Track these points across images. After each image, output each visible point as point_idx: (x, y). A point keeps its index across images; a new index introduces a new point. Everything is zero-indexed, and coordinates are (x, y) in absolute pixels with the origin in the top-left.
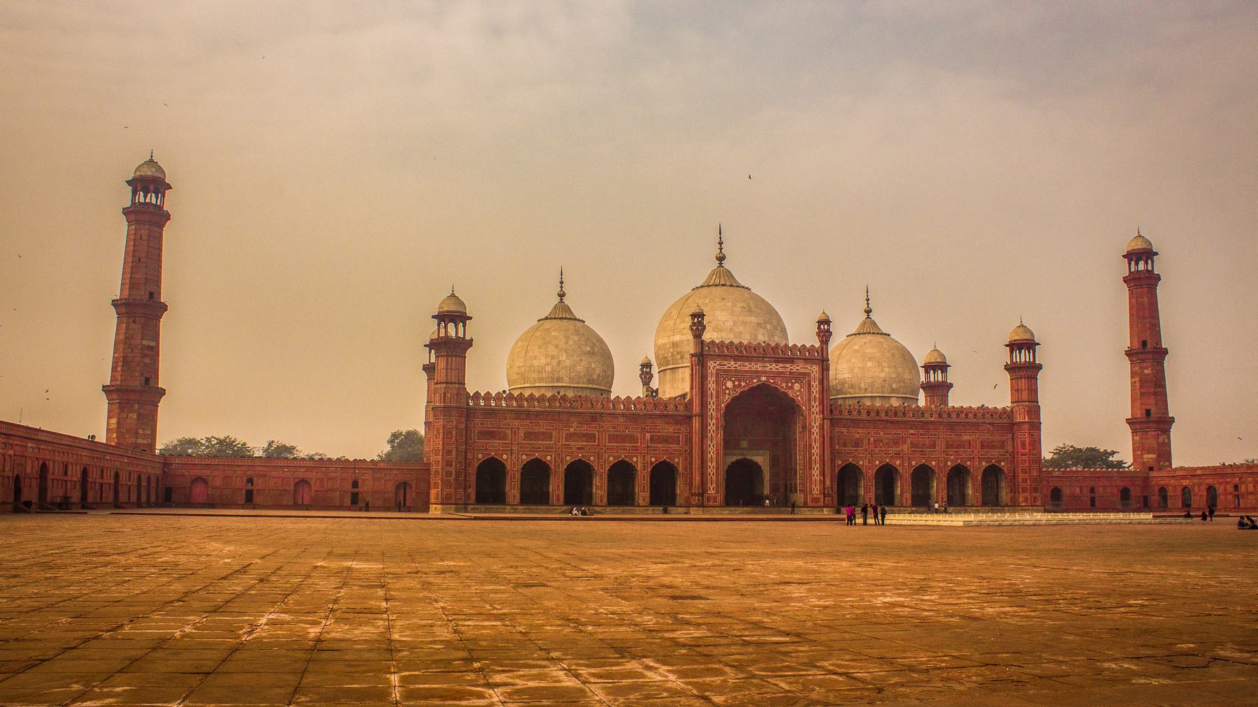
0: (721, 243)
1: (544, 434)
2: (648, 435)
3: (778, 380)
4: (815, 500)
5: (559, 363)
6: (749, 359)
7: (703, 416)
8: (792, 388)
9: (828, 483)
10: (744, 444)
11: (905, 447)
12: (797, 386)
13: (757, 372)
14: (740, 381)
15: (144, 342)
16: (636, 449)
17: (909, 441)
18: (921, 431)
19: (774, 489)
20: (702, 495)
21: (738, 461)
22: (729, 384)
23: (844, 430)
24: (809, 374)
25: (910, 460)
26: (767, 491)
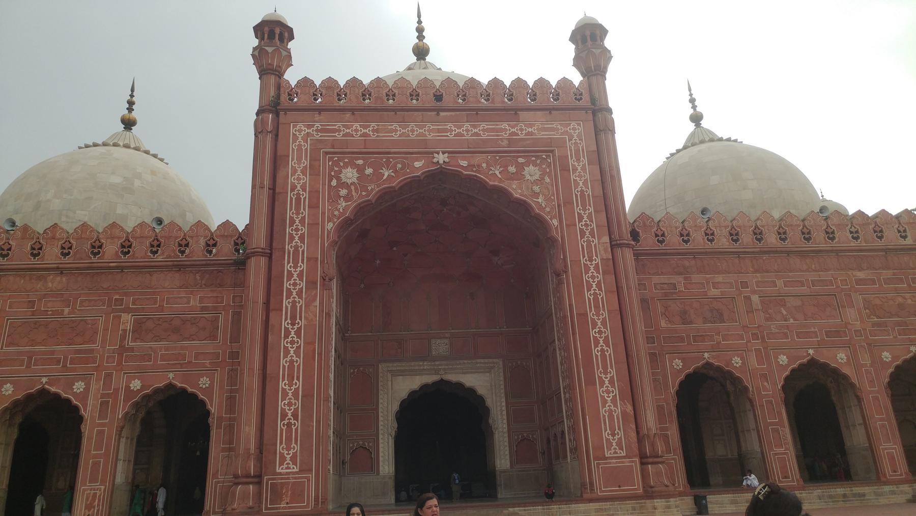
2: (127, 320)
3: (477, 159)
5: (37, 207)
6: (401, 113)
7: (271, 253)
8: (518, 176)
9: (650, 420)
10: (440, 347)
12: (532, 172)
13: (425, 143)
14: (377, 168)
17: (858, 299)
18: (887, 274)
19: (522, 449)
21: (424, 387)
22: (350, 175)
23: (679, 280)
26: (502, 460)
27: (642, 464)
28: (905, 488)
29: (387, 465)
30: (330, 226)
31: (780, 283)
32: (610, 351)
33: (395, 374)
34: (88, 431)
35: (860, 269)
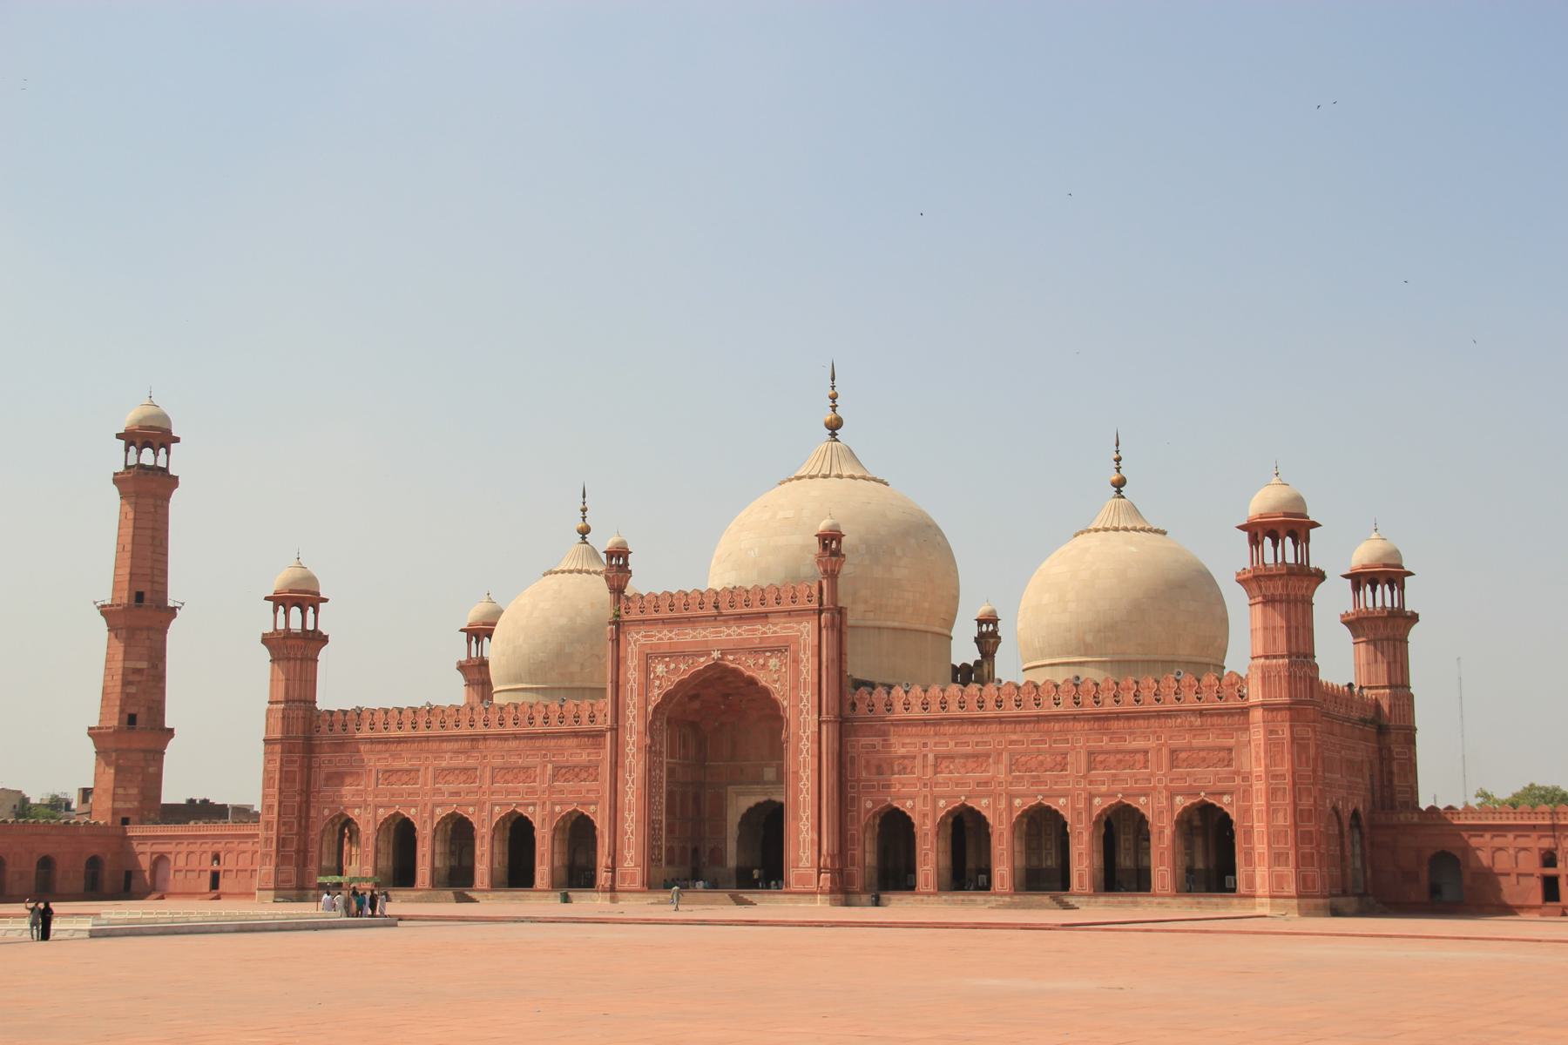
0: (834, 398)
1: (408, 771)
4: (801, 879)
6: (691, 621)
11: (998, 771)
12: (773, 662)
15: (131, 665)
16: (533, 791)
17: (1005, 756)
18: (1035, 736)
20: (613, 869)
21: (758, 805)
22: (660, 669)
23: (877, 741)
24: (796, 639)
25: (1011, 797)
27: (819, 873)
28: (1007, 899)
29: (732, 862)
30: (650, 709)
31: (951, 744)
32: (809, 798)
33: (738, 794)
34: (538, 834)
35: (1014, 732)
